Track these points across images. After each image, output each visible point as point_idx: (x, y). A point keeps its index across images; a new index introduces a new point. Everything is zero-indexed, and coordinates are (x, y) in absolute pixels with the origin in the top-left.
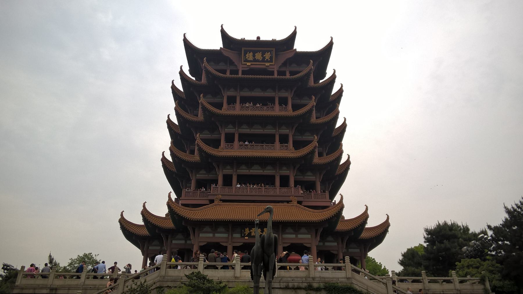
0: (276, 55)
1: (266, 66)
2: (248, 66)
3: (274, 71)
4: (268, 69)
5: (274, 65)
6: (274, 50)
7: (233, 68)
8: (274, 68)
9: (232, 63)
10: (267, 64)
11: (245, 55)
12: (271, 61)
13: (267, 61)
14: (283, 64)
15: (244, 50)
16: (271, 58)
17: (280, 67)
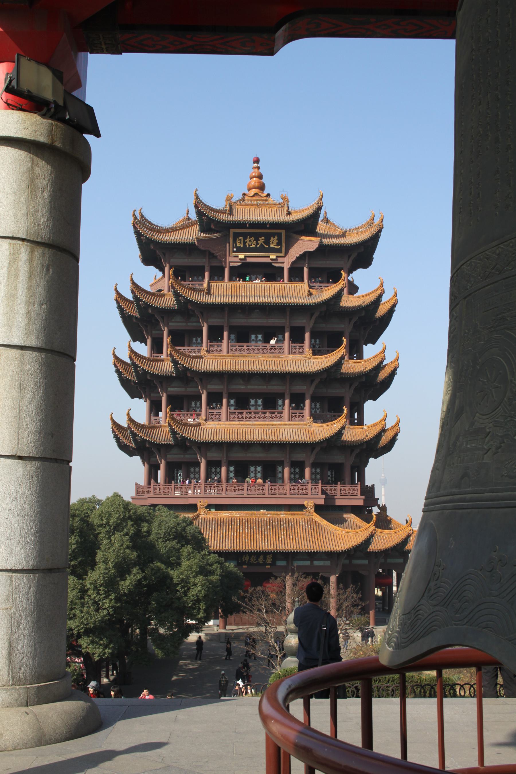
0: (288, 238)
1: (272, 260)
2: (240, 259)
3: (282, 269)
4: (273, 264)
5: (284, 257)
6: (283, 232)
7: (215, 264)
8: (283, 263)
9: (212, 256)
10: (273, 256)
11: (235, 241)
12: (279, 251)
13: (273, 251)
14: (298, 258)
15: (234, 233)
16: (279, 243)
17: (293, 263)
